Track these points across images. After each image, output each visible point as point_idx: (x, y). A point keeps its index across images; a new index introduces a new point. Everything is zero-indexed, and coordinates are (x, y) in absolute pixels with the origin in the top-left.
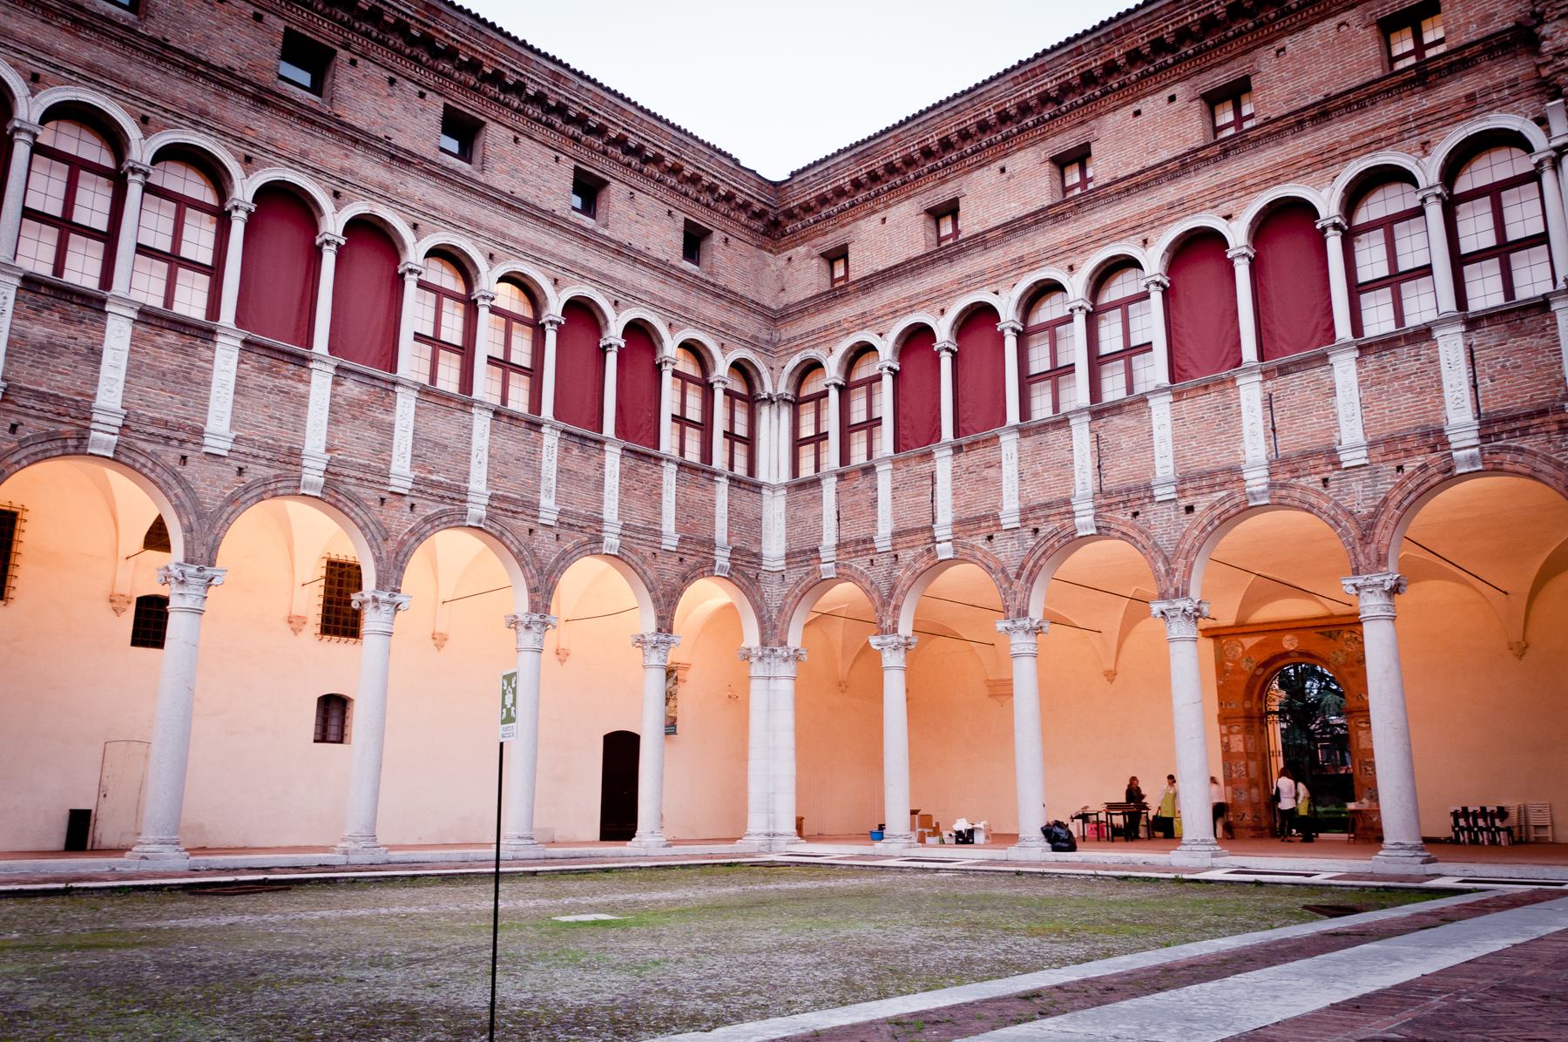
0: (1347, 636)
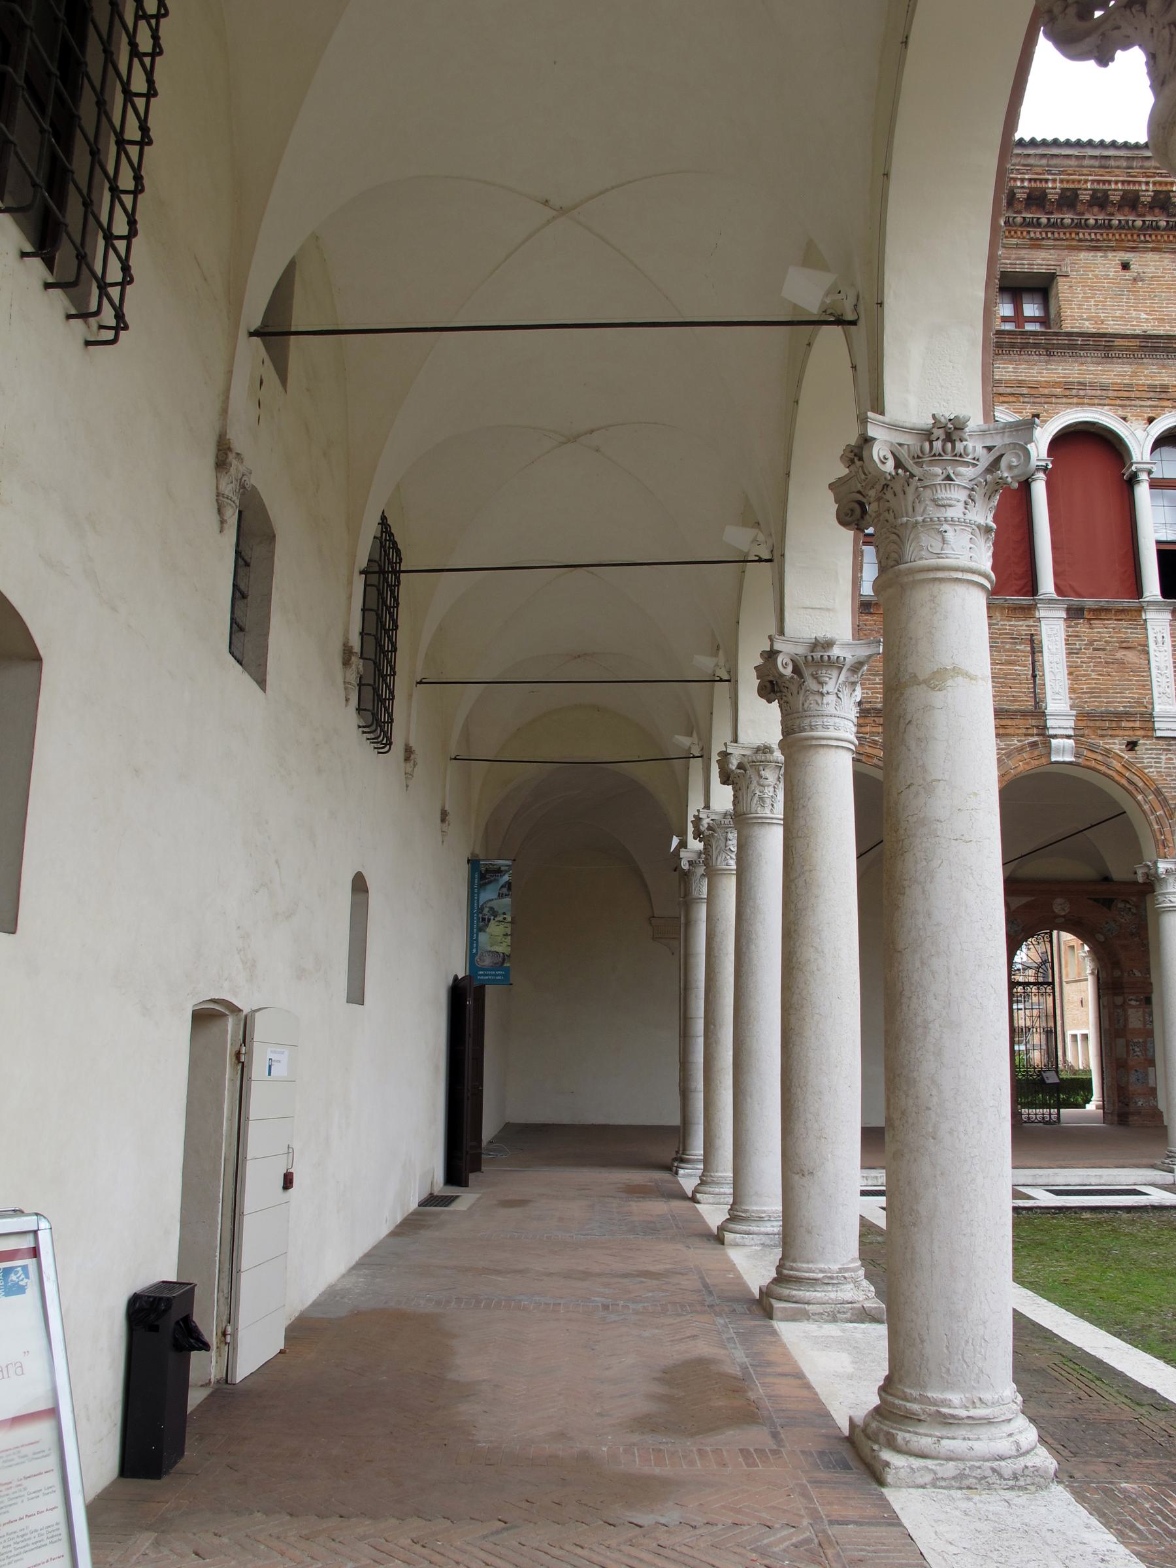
0: (1121, 905)
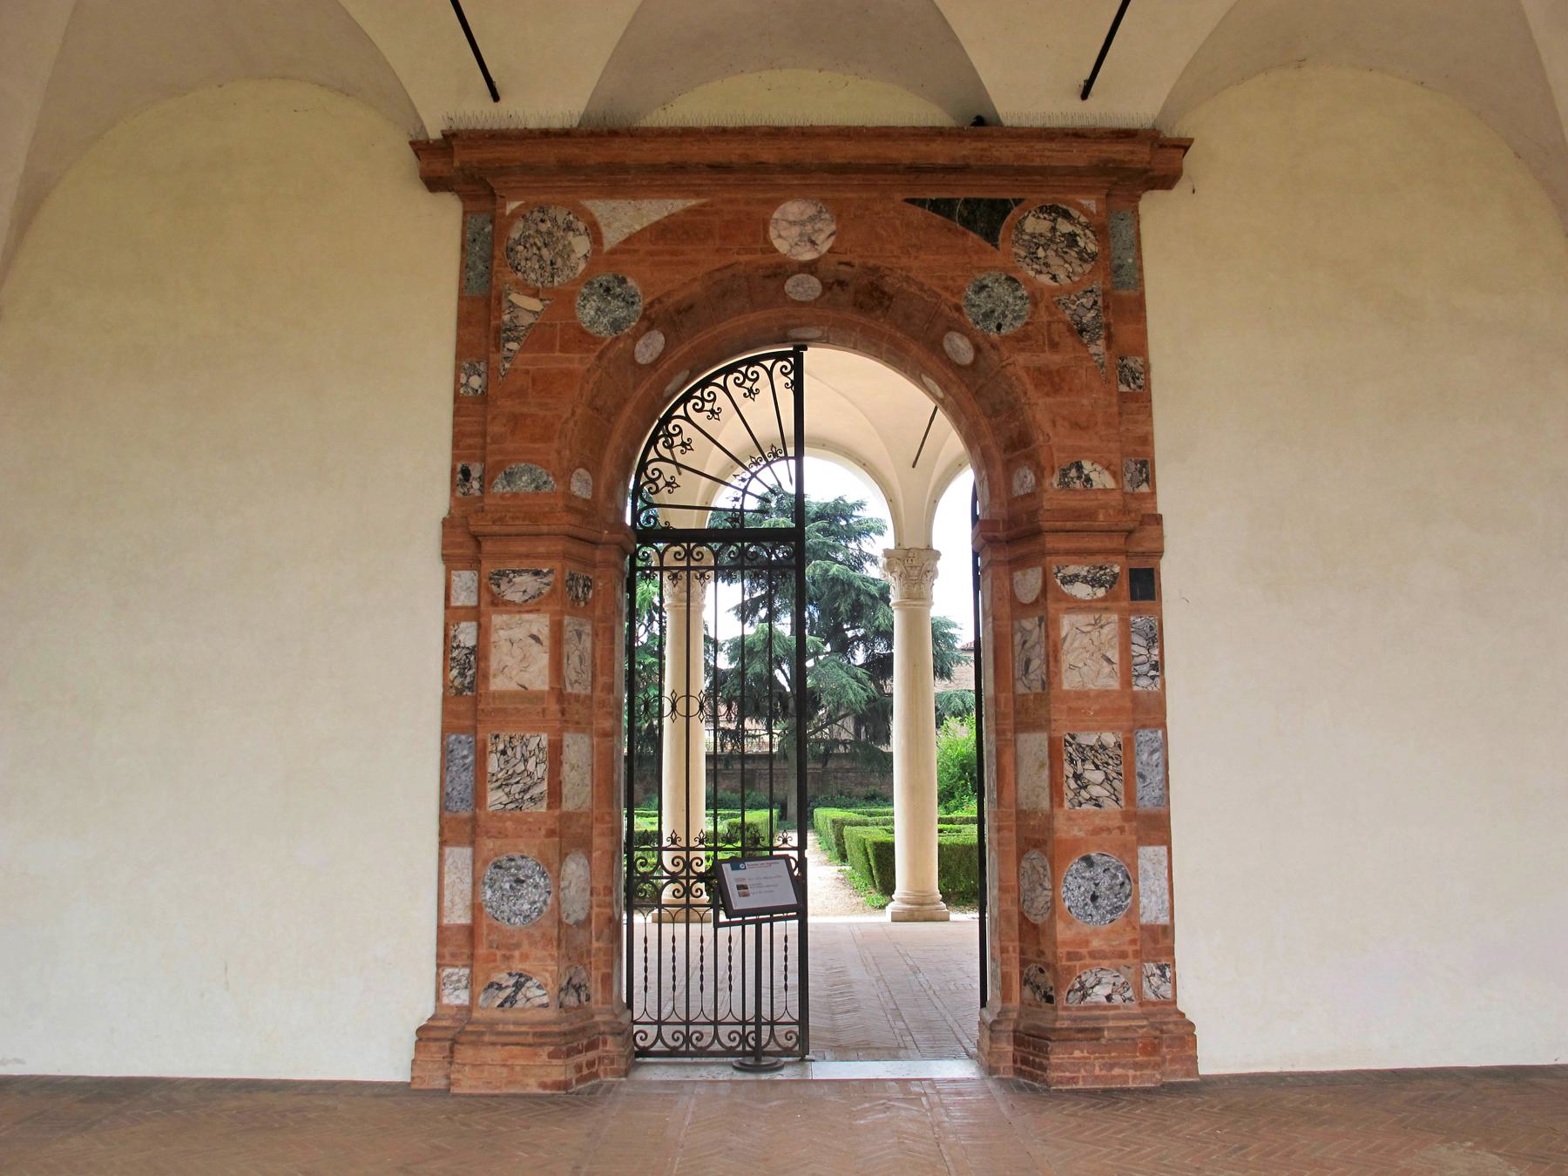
0: (1035, 225)
